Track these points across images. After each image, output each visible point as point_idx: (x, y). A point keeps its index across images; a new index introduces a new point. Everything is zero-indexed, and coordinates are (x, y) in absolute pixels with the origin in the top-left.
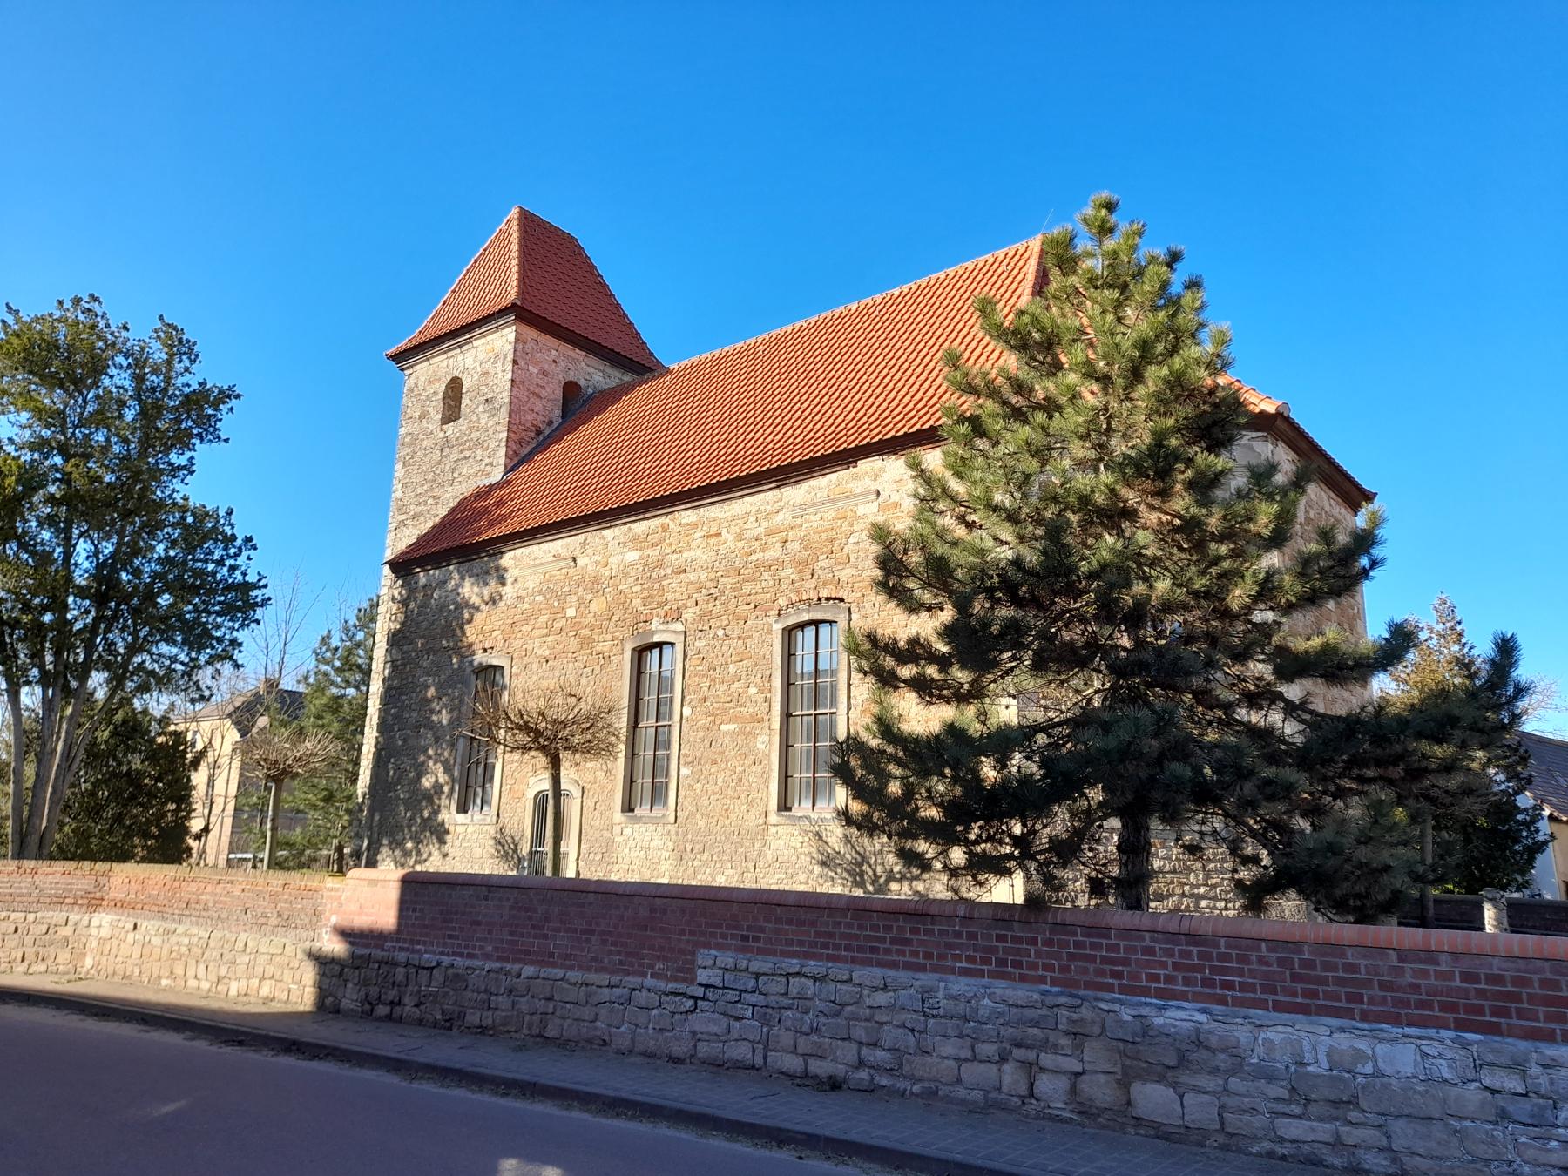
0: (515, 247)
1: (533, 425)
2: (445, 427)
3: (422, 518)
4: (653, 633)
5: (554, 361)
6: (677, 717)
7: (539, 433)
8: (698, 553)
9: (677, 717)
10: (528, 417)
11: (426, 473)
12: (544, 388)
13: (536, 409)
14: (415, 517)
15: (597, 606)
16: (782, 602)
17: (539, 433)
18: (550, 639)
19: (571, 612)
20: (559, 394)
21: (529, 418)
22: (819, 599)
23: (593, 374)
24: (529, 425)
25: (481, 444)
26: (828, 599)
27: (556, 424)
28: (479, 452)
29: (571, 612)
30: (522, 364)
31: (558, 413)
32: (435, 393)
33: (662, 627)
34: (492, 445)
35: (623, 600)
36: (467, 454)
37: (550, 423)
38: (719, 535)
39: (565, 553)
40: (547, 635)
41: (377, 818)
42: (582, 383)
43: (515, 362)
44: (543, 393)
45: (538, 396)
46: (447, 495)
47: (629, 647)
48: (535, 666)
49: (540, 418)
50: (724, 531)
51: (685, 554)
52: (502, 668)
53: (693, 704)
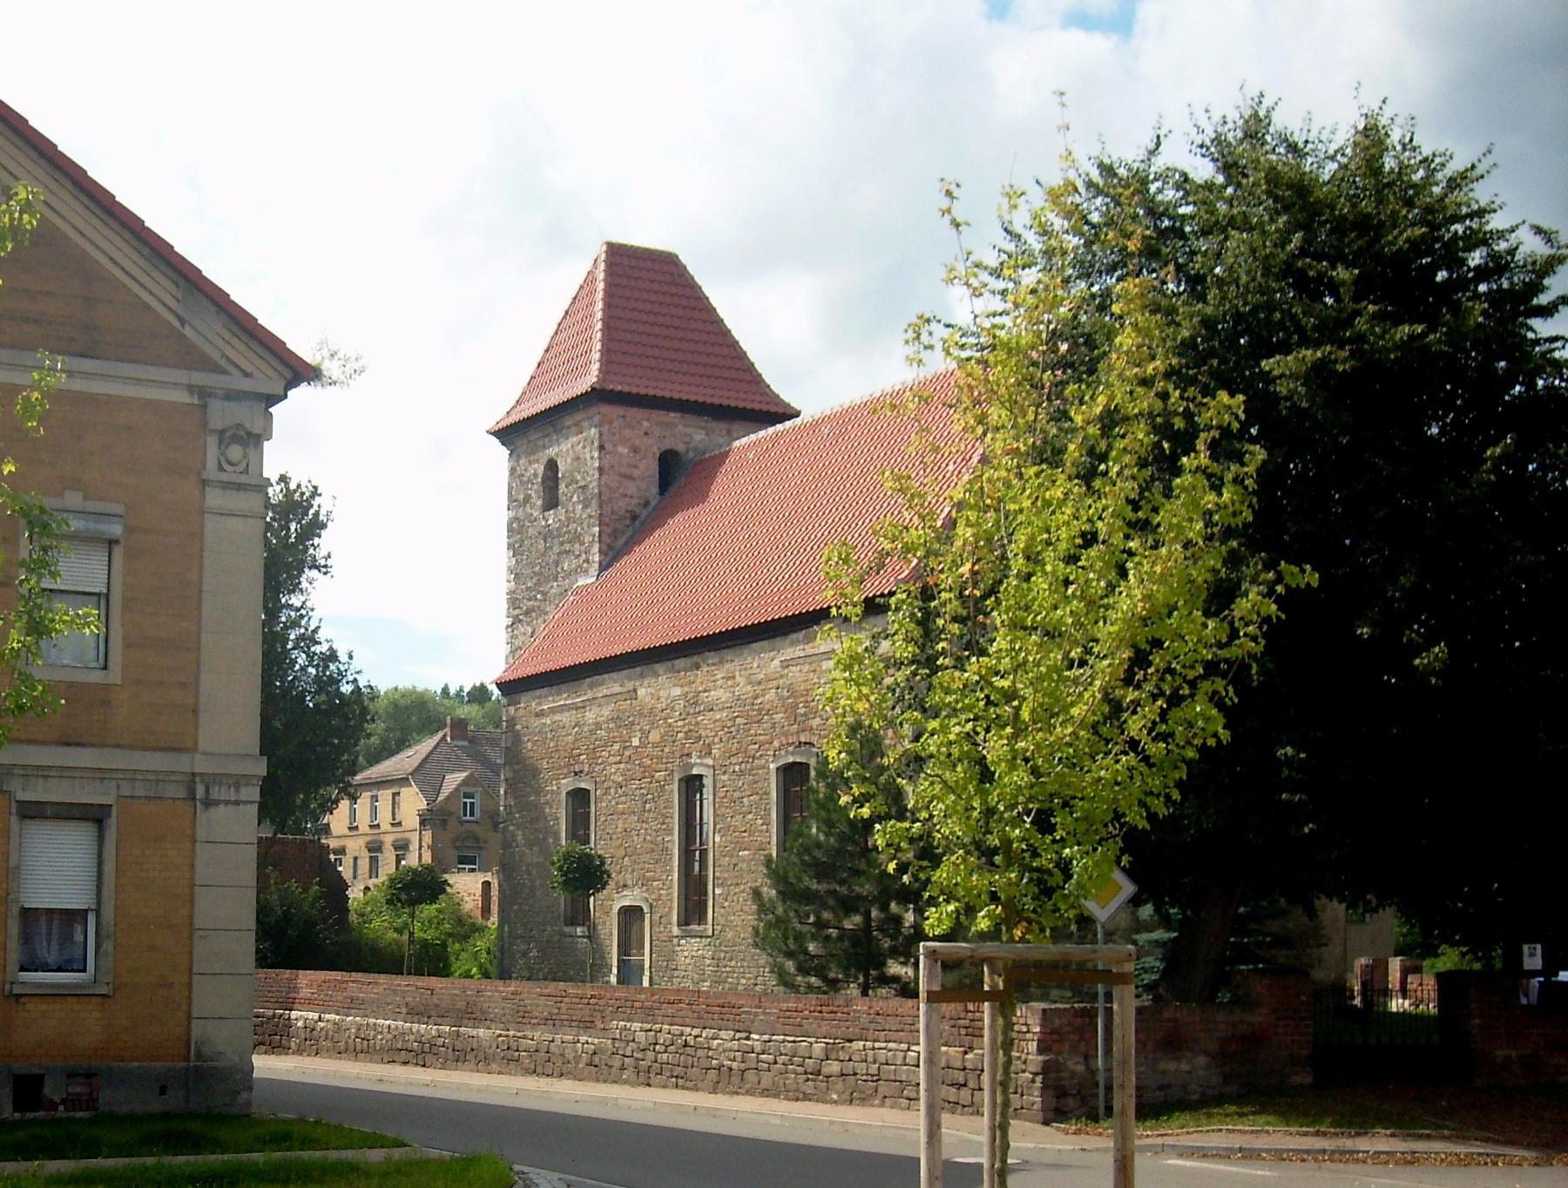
0: (600, 295)
1: (627, 511)
2: (546, 514)
3: (534, 614)
4: (693, 766)
5: (646, 433)
6: (711, 844)
7: (634, 517)
8: (720, 695)
9: (711, 844)
10: (620, 503)
11: (534, 565)
12: (636, 467)
13: (629, 492)
14: (527, 613)
15: (654, 736)
16: (776, 744)
17: (634, 517)
18: (622, 766)
19: (636, 742)
20: (654, 467)
21: (621, 506)
22: (800, 743)
23: (690, 435)
24: (622, 512)
25: (577, 538)
26: (806, 743)
27: (653, 504)
28: (577, 546)
29: (636, 742)
30: (608, 446)
31: (655, 490)
32: (536, 475)
33: (698, 761)
34: (587, 539)
35: (669, 736)
36: (567, 547)
37: (646, 504)
38: (734, 677)
39: (631, 688)
40: (620, 763)
41: (506, 929)
42: (681, 448)
43: (601, 448)
44: (636, 473)
45: (630, 478)
46: (554, 591)
47: (677, 777)
48: (612, 791)
49: (635, 501)
50: (737, 676)
51: (712, 693)
52: (589, 791)
53: (723, 831)
